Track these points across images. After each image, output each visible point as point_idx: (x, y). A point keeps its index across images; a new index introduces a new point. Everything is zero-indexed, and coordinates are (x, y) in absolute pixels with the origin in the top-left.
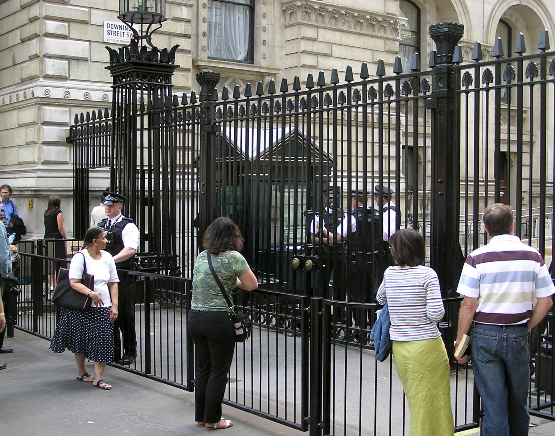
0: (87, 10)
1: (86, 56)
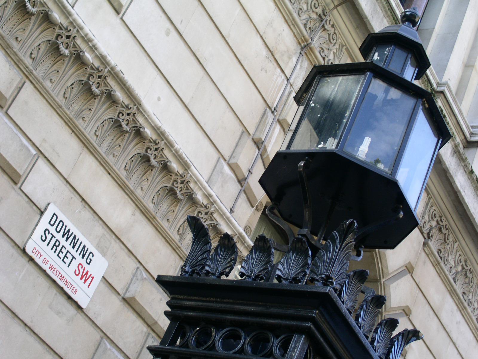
0: (34, 152)
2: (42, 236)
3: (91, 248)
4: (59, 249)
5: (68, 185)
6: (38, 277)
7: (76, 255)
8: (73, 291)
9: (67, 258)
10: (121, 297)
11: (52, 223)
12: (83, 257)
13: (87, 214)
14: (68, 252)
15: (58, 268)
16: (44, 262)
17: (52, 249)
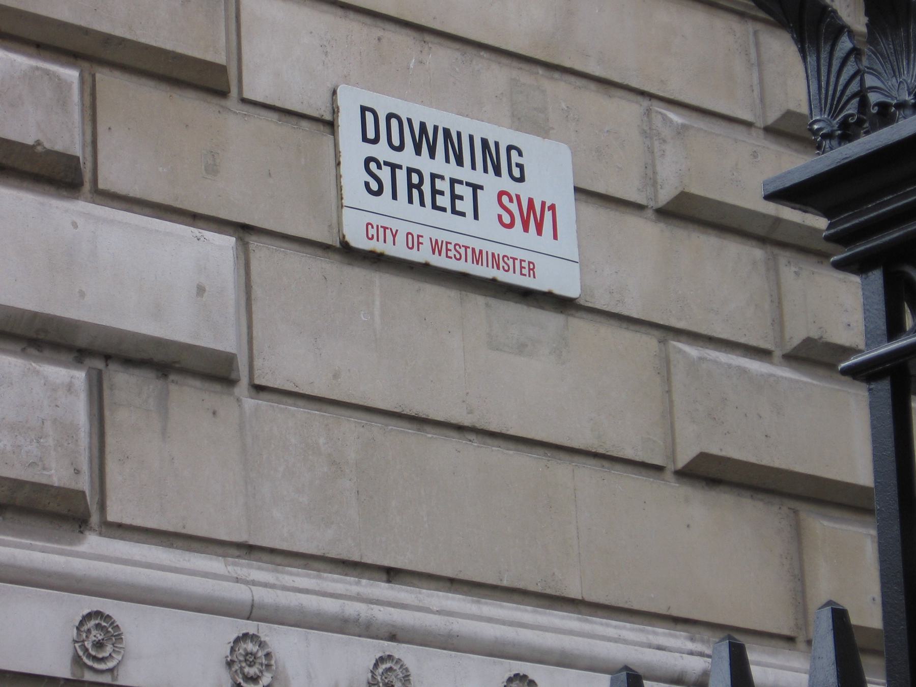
1: (227, 341)
2: (367, 185)
3: (502, 135)
4: (426, 188)
5: (352, 15)
6: (418, 291)
7: (478, 177)
8: (525, 271)
9: (461, 198)
10: (650, 213)
11: (371, 135)
12: (498, 173)
13: (442, 57)
14: (453, 182)
15: (454, 239)
16: (410, 245)
17: (410, 201)
